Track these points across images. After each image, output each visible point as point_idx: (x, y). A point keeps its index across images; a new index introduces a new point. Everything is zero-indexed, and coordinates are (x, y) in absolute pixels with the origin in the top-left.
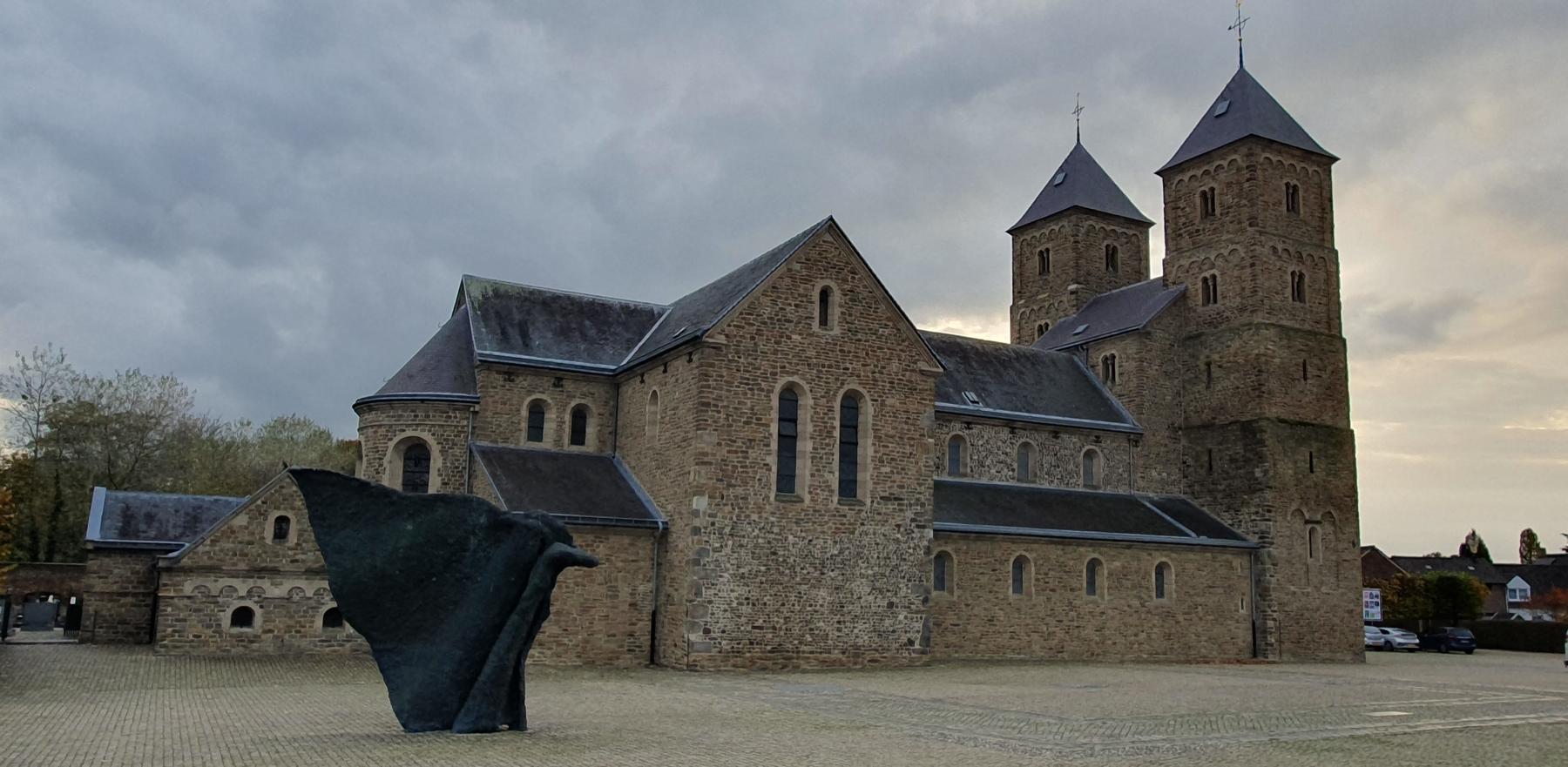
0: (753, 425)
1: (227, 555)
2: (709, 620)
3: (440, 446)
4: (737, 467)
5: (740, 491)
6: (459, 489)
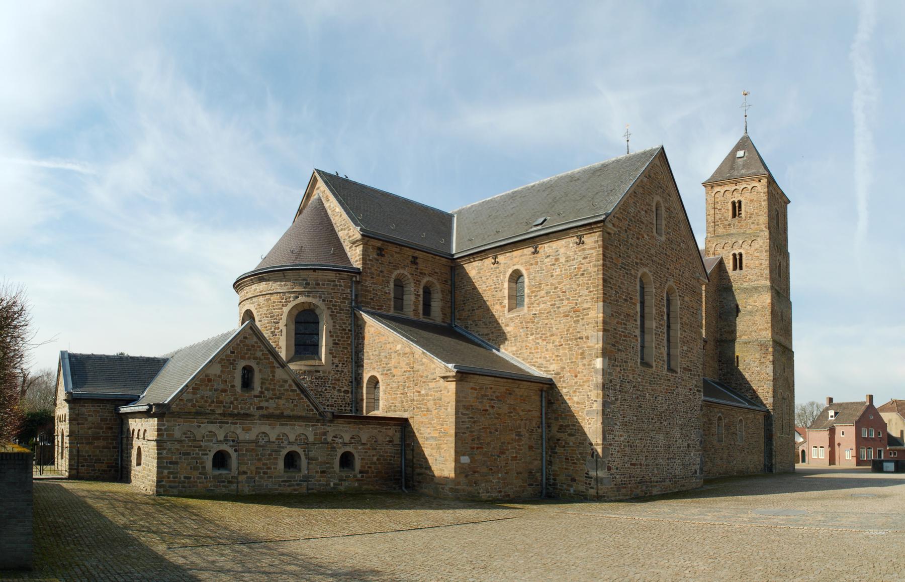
1: (206, 401)
2: (610, 459)
3: (330, 311)
5: (623, 355)
6: (347, 348)
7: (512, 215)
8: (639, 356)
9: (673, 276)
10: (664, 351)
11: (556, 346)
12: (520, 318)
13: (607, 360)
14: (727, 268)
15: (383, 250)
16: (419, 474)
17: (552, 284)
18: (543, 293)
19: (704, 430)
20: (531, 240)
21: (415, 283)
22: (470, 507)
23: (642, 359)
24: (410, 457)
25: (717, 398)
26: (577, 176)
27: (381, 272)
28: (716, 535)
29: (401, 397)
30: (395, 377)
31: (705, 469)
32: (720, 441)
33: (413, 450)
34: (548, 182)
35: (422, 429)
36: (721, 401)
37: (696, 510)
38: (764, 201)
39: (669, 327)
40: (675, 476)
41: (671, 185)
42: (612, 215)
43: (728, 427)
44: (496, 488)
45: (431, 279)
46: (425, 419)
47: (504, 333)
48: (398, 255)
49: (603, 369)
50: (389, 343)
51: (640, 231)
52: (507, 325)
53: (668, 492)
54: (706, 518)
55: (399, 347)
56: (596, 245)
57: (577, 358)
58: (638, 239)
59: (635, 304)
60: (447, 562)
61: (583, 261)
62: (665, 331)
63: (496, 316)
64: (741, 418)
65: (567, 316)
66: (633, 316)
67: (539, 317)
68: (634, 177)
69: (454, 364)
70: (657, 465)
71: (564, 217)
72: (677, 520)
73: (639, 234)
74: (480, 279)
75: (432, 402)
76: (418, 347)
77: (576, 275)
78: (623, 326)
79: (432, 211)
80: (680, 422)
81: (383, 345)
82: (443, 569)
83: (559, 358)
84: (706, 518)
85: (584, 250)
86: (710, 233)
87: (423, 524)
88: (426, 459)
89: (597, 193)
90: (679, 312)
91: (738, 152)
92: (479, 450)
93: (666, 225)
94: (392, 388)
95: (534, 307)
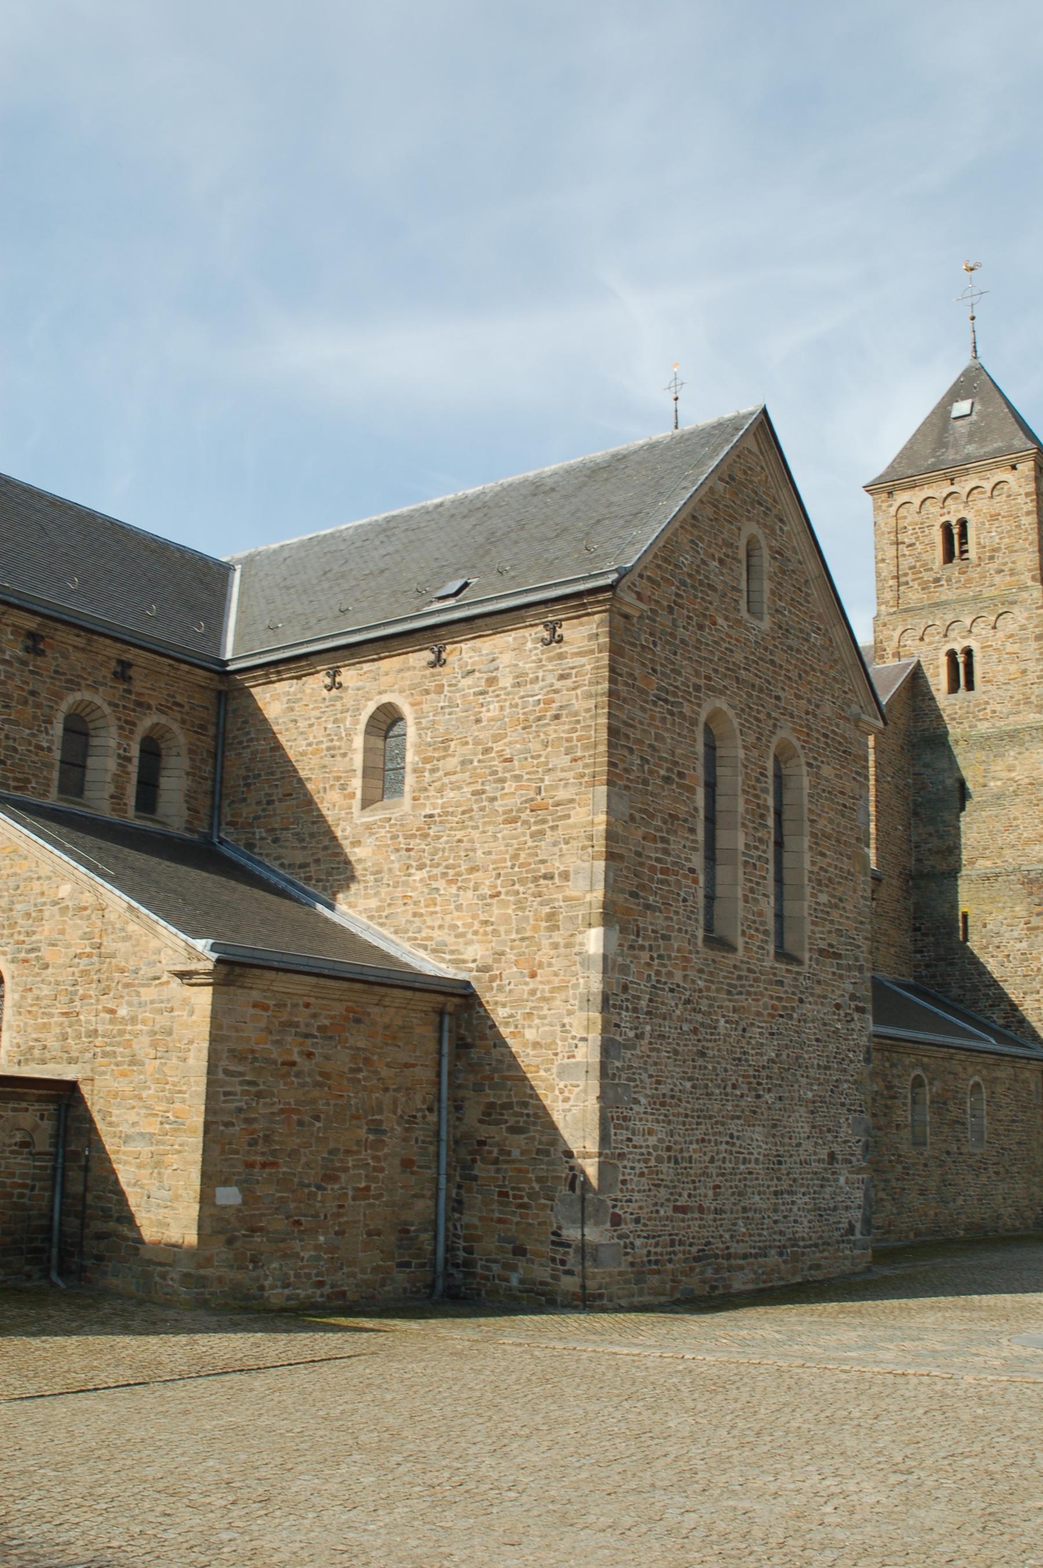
0: (674, 786)
2: (620, 1195)
4: (652, 869)
7: (382, 572)
8: (702, 922)
9: (792, 716)
10: (768, 906)
11: (482, 897)
12: (391, 826)
13: (615, 934)
14: (933, 688)
15: (43, 638)
16: (100, 1236)
17: (477, 742)
18: (452, 763)
19: (874, 1115)
20: (428, 633)
21: (121, 728)
22: (235, 1327)
23: (709, 928)
24: (77, 1188)
25: (908, 1027)
26: (550, 483)
27: (33, 693)
28: (910, 1405)
29: (61, 1024)
30: (50, 970)
31: (878, 1220)
32: (919, 1142)
33: (86, 1169)
34: (478, 497)
35: (115, 1112)
36: (921, 1036)
37: (853, 1334)
38: (1028, 513)
39: (779, 844)
40: (794, 1241)
41: (785, 495)
42: (637, 571)
43: (940, 1103)
44: (308, 1276)
45: (163, 720)
46: (122, 1085)
47: (348, 862)
48: (80, 655)
49: (605, 957)
50: (39, 878)
51: (707, 609)
52: (357, 843)
53: (775, 1283)
54: (882, 1355)
55: (65, 890)
56: (593, 645)
57: (536, 929)
58: (701, 627)
59: (692, 790)
60: (160, 1485)
61: (558, 685)
62: (770, 855)
63: (330, 819)
64: (977, 1078)
65: (514, 820)
66: (686, 820)
67: (441, 822)
68: (693, 483)
69: (211, 941)
70: (745, 1210)
71: (513, 577)
72: (800, 1362)
73: (705, 615)
74: (291, 725)
75: (146, 1040)
76: (118, 892)
77: (539, 719)
78: (659, 845)
79: (178, 555)
80: (810, 1095)
81: (22, 884)
82: (147, 1505)
83: (489, 929)
84: (882, 1355)
85: (561, 656)
86: (886, 603)
87: (103, 1375)
88: (121, 1193)
89: (599, 521)
90: (806, 805)
91: (956, 405)
92: (267, 1170)
93: (773, 593)
94: (38, 998)
95: (427, 798)
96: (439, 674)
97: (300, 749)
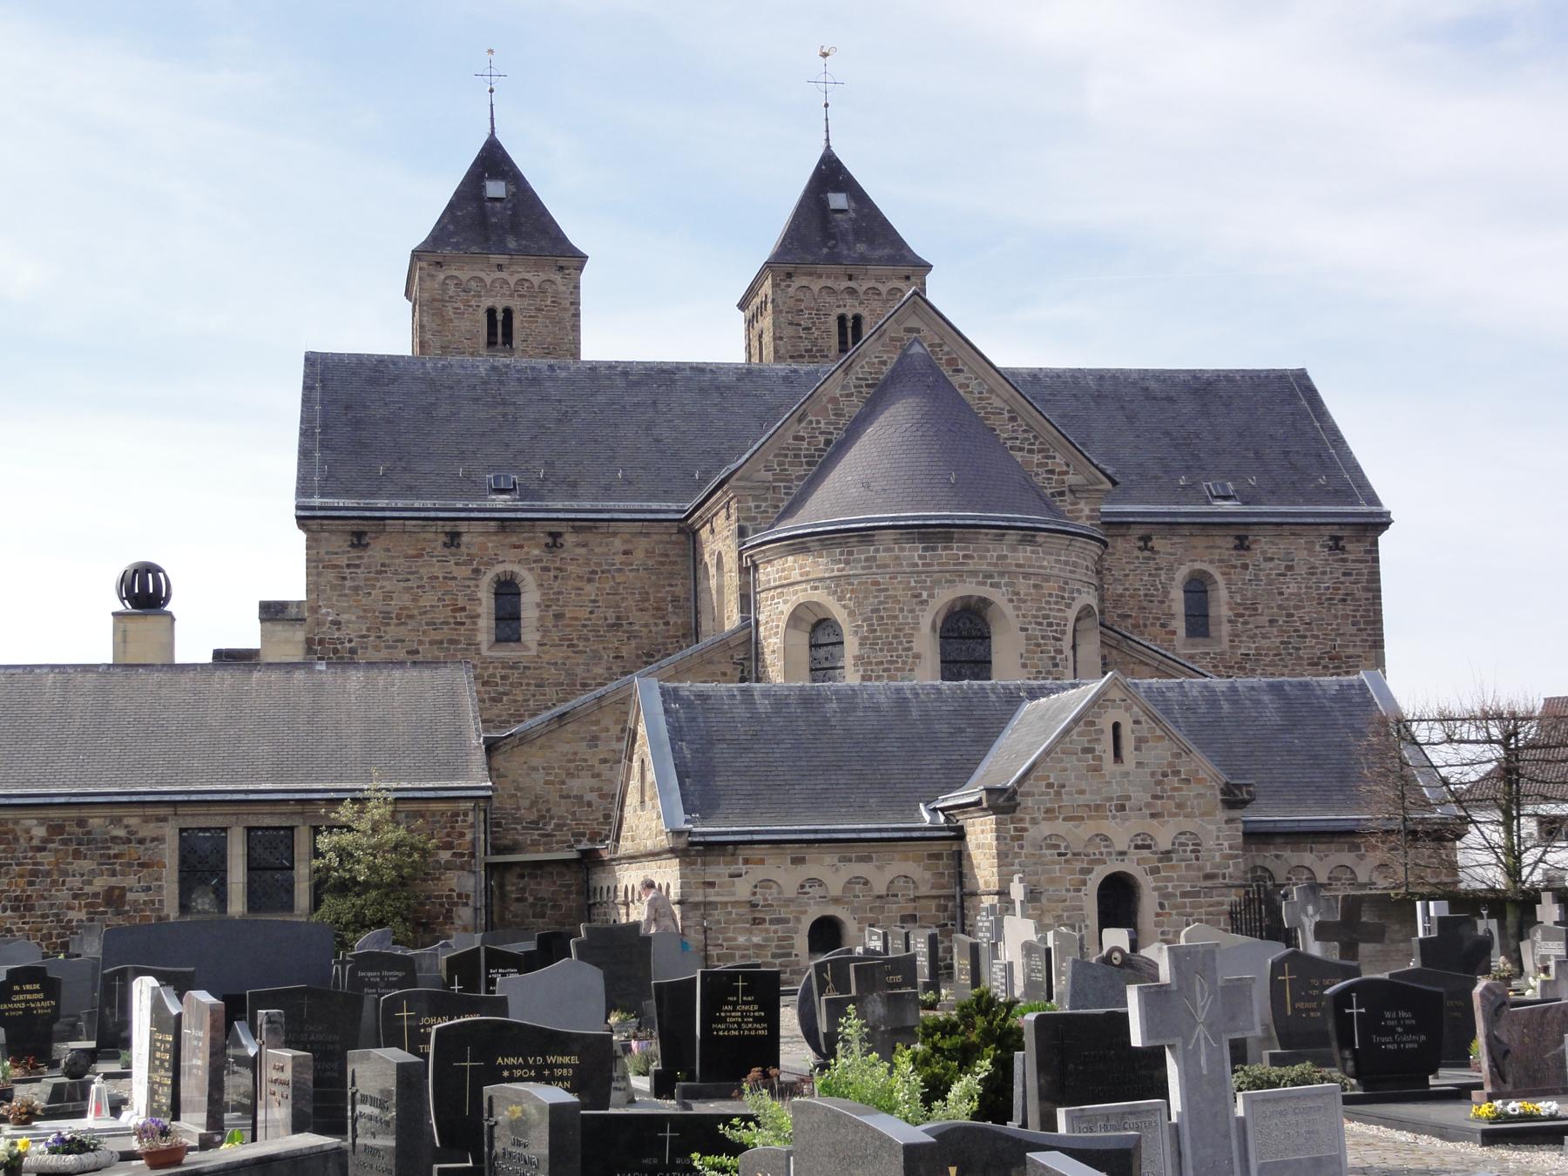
61: (1342, 579)
77: (1331, 599)
95: (1241, 642)
96: (1244, 556)
97: (1118, 592)
